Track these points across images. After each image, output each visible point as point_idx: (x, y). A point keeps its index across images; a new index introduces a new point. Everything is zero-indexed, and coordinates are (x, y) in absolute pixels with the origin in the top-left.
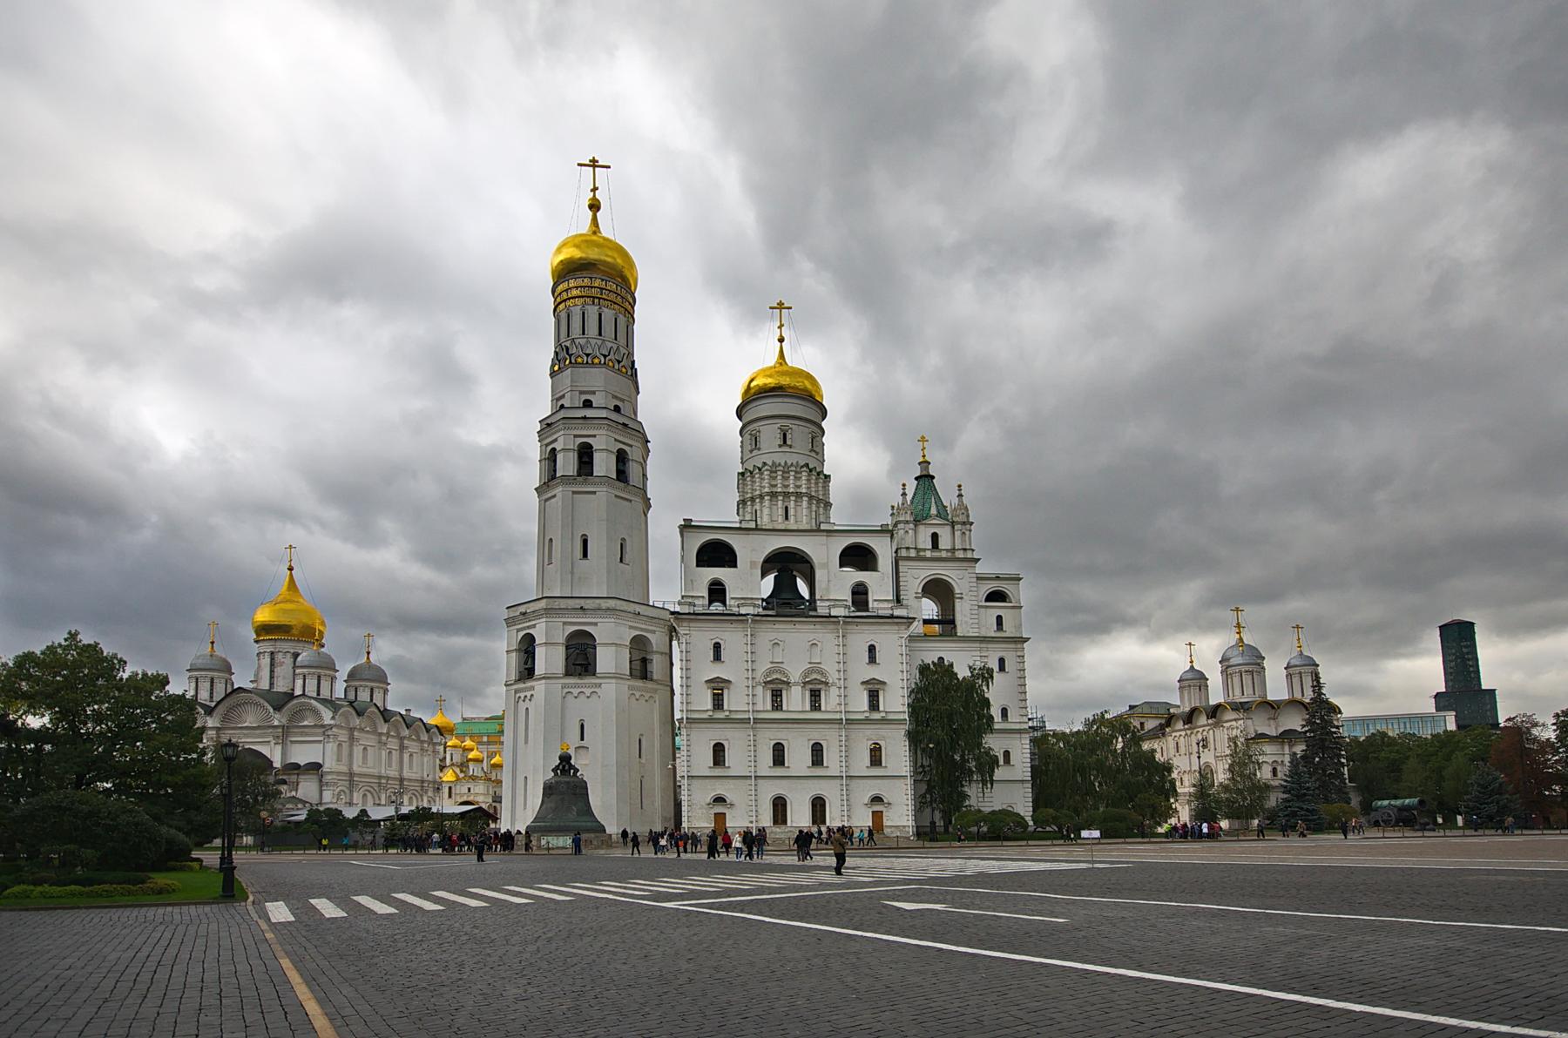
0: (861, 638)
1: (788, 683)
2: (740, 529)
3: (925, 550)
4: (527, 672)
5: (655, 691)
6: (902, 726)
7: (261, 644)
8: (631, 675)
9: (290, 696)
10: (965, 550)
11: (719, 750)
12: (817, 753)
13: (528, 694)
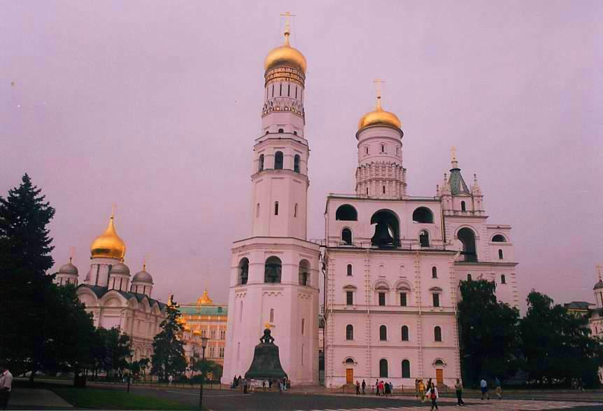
0: (428, 263)
1: (388, 289)
2: (357, 199)
3: (458, 211)
4: (244, 280)
5: (311, 293)
6: (453, 316)
7: (94, 260)
8: (300, 283)
9: (105, 290)
10: (480, 211)
11: (350, 328)
12: (405, 331)
13: (243, 293)
